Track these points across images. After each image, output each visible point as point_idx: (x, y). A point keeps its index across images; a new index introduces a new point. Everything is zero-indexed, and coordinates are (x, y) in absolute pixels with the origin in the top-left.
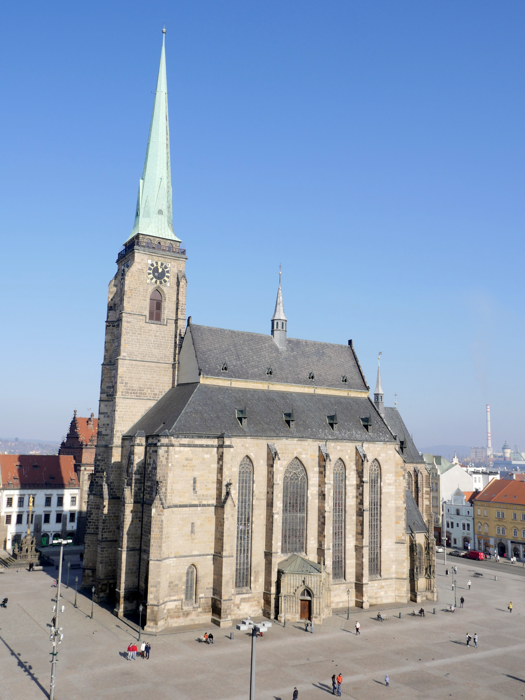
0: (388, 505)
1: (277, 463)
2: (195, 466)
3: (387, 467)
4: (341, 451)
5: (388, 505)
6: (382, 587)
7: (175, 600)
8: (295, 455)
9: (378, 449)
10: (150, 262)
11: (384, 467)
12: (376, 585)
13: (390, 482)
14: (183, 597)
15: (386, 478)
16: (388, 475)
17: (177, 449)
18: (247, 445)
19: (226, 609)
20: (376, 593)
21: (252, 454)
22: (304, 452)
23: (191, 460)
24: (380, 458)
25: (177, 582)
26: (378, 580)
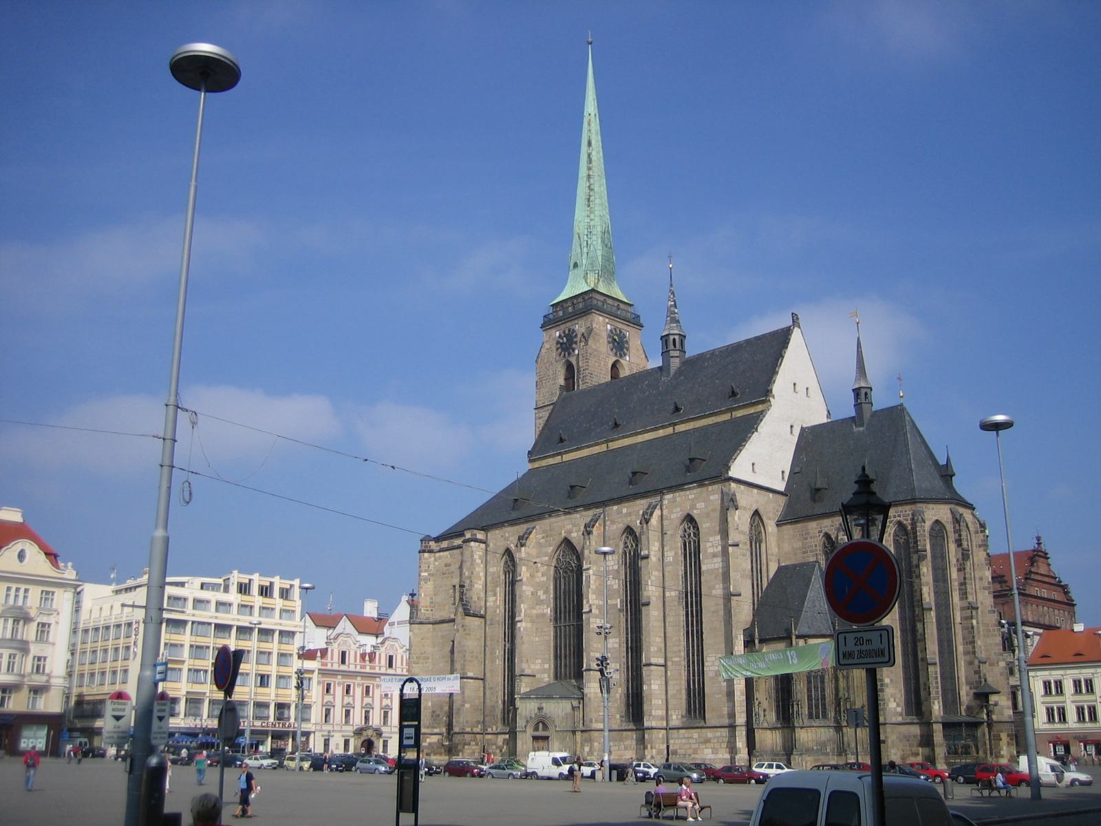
0: (714, 592)
1: (520, 551)
2: (453, 573)
3: (708, 525)
4: (629, 514)
5: (714, 592)
6: (707, 741)
7: (436, 734)
8: (563, 535)
9: (690, 497)
10: (558, 334)
11: (704, 526)
12: (696, 736)
13: (716, 550)
14: (444, 730)
15: (709, 544)
16: (711, 539)
17: (437, 555)
18: (507, 535)
19: (457, 744)
20: (695, 752)
21: (512, 545)
22: (574, 529)
23: (450, 565)
24: (695, 511)
25: (438, 712)
26: (697, 728)
